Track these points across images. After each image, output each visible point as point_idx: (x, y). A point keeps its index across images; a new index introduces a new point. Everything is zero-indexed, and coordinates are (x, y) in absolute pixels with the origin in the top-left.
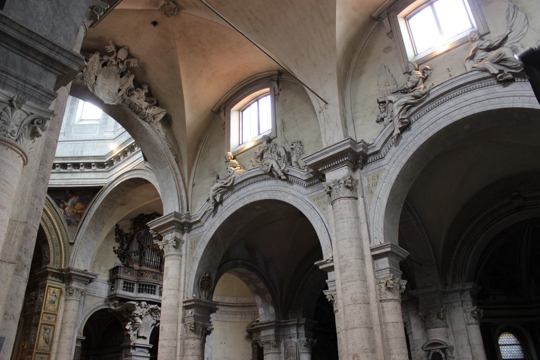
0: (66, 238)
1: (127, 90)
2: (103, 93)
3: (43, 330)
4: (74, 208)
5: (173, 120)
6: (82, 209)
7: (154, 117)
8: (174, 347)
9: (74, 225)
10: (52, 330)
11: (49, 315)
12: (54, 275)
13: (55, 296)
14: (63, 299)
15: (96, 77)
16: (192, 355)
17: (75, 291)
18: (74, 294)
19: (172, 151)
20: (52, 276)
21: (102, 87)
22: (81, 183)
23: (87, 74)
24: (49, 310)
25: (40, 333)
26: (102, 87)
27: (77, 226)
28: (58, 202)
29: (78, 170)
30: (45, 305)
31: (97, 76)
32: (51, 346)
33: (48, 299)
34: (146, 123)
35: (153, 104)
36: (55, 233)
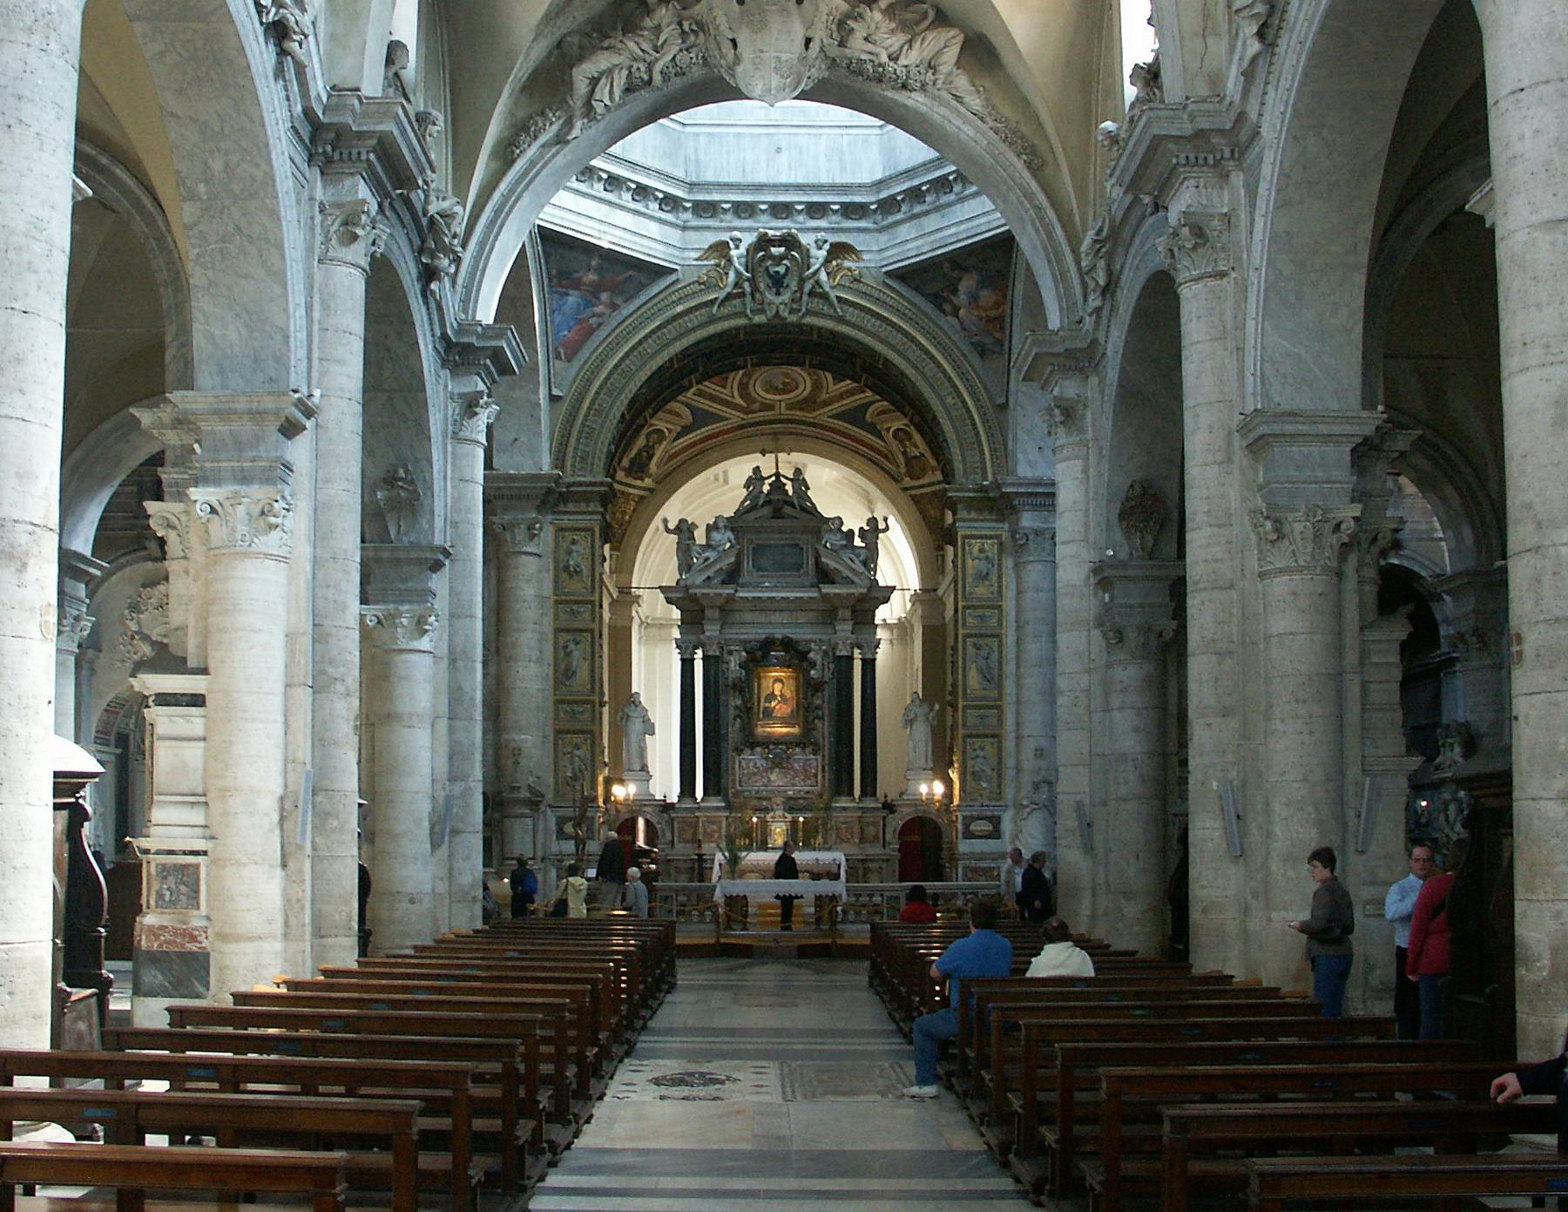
0: (984, 396)
1: (834, 27)
2: (763, 77)
3: (971, 650)
4: (978, 307)
5: (998, 47)
6: (998, 304)
7: (932, 66)
8: (1082, 691)
9: (993, 352)
10: (995, 648)
11: (980, 612)
12: (971, 504)
13: (987, 558)
14: (1008, 563)
15: (734, 41)
16: (1120, 708)
17: (1031, 537)
18: (1032, 545)
19: (1011, 144)
20: (969, 508)
21: (757, 60)
22: (965, 235)
23: (712, 45)
24: (978, 599)
25: (964, 660)
26: (757, 60)
27: (1001, 354)
28: (937, 300)
29: (952, 197)
30: (964, 587)
31: (735, 36)
32: (1000, 686)
33: (970, 571)
34: (913, 95)
35: (926, 23)
36: (950, 389)
